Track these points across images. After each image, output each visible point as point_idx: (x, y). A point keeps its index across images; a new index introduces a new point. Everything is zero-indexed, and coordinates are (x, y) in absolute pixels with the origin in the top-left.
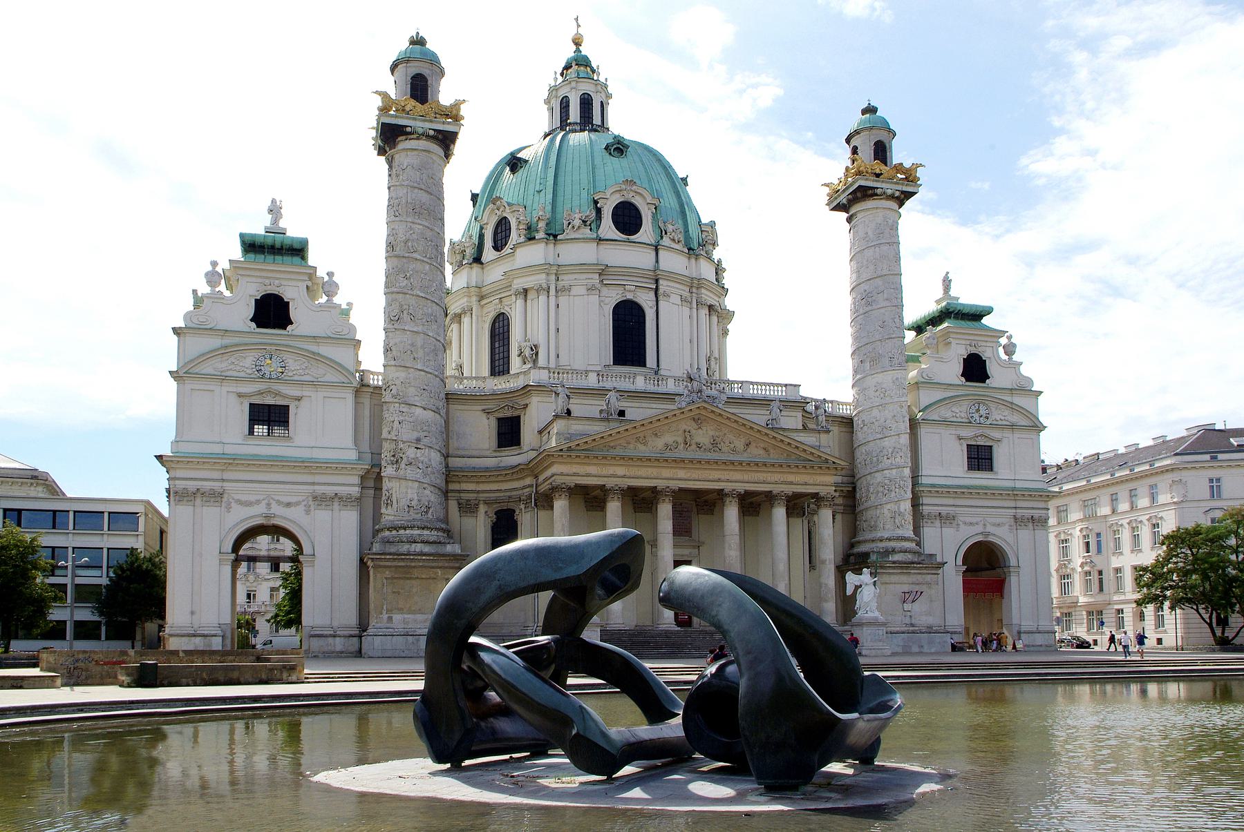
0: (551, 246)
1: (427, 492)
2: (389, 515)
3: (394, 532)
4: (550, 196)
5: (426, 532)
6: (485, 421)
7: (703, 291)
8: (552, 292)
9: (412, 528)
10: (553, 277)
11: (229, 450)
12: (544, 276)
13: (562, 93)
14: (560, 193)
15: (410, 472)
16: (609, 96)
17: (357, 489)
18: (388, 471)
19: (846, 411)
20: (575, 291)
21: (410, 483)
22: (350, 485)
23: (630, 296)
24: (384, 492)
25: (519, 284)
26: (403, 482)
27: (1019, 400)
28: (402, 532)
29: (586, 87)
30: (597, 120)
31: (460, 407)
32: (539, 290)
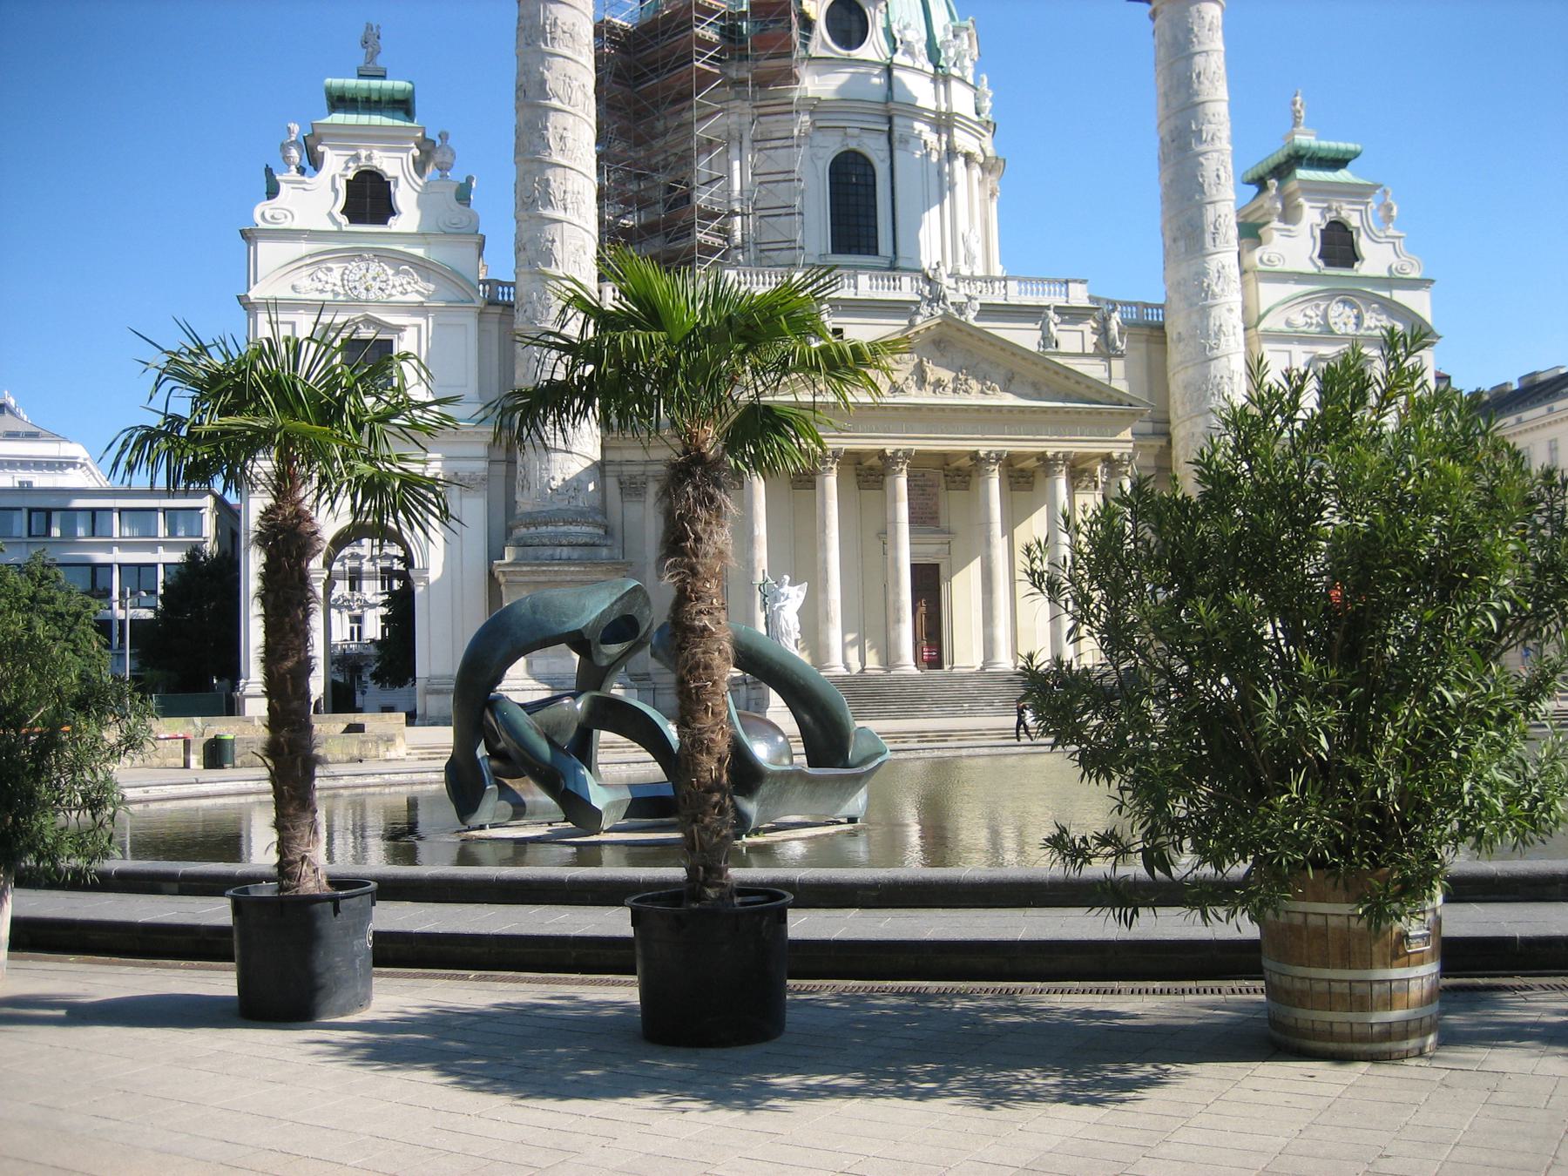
5: (573, 529)
17: (483, 465)
19: (1153, 316)
23: (853, 145)
24: (519, 469)
27: (1400, 296)
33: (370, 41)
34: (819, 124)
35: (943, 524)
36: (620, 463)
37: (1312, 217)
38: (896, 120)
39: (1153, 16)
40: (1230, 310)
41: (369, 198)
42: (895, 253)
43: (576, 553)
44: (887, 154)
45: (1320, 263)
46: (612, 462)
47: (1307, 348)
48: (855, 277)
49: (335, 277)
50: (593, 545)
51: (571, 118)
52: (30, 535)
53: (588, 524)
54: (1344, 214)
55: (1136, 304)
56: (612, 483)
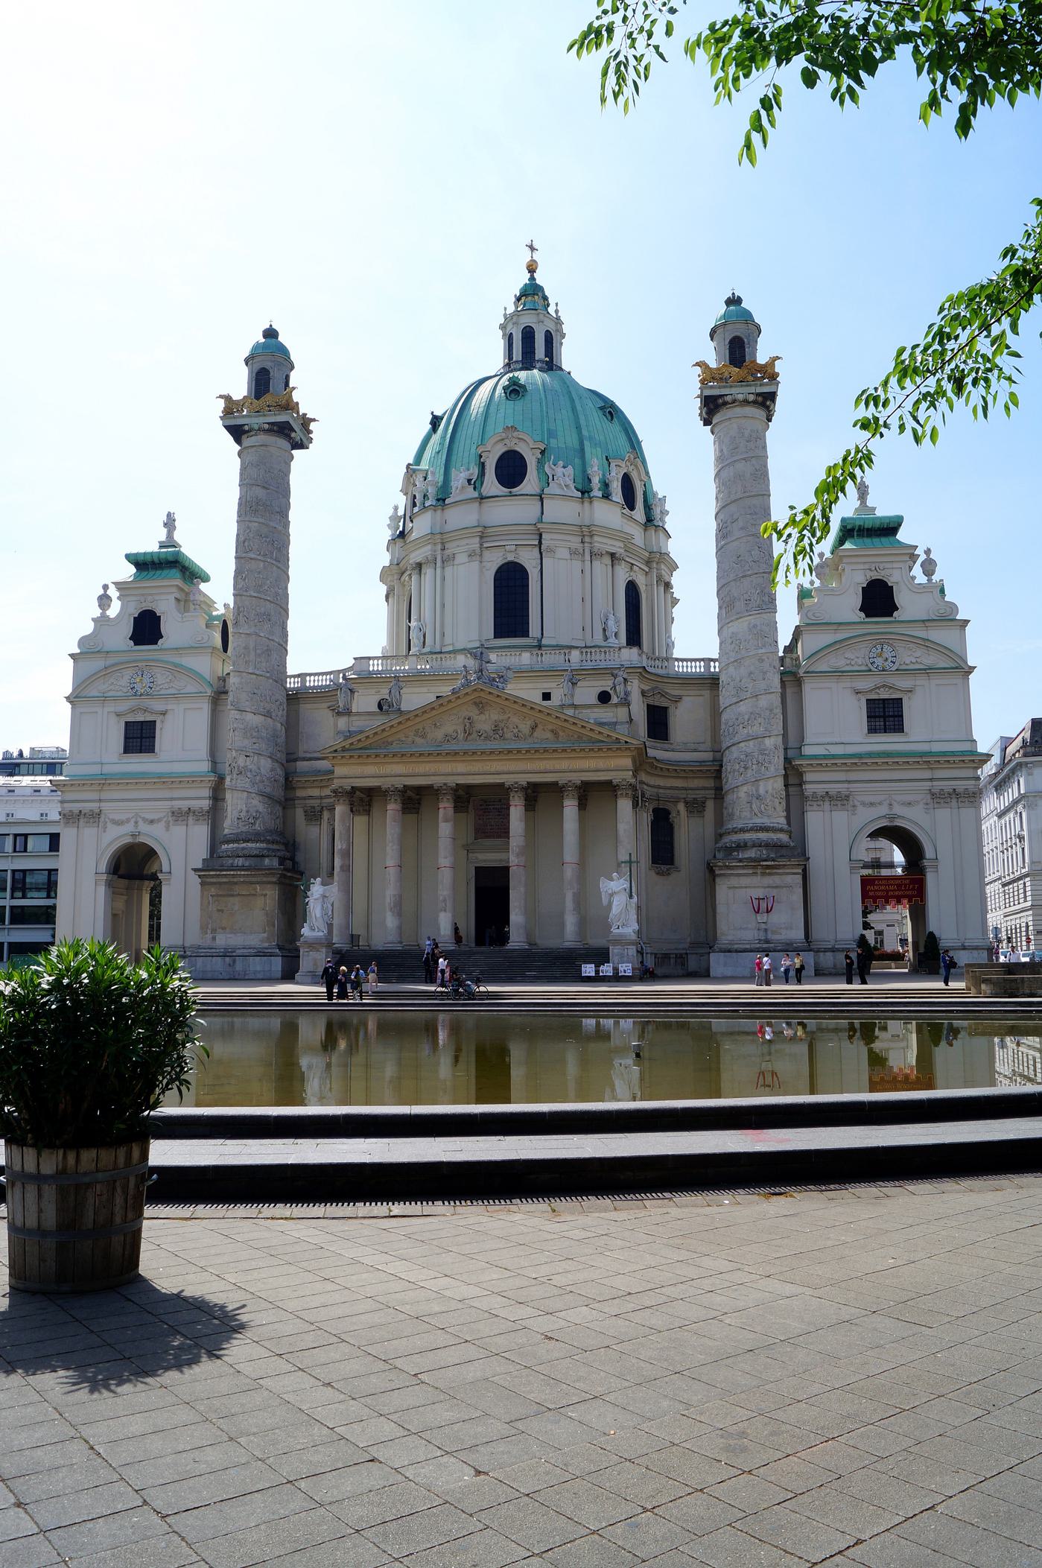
0: (439, 512)
2: (228, 826)
7: (596, 538)
8: (439, 564)
10: (439, 547)
11: (107, 769)
12: (429, 547)
13: (508, 332)
14: (455, 452)
15: (243, 782)
16: (558, 321)
19: (715, 668)
20: (461, 558)
23: (511, 558)
25: (416, 556)
26: (236, 794)
27: (937, 635)
29: (528, 320)
31: (308, 706)
32: (428, 562)
33: (170, 523)
36: (305, 798)
37: (858, 578)
40: (761, 661)
41: (147, 628)
45: (863, 615)
46: (299, 798)
47: (849, 685)
49: (124, 681)
52: (15, 851)
53: (262, 842)
54: (883, 573)
56: (299, 813)
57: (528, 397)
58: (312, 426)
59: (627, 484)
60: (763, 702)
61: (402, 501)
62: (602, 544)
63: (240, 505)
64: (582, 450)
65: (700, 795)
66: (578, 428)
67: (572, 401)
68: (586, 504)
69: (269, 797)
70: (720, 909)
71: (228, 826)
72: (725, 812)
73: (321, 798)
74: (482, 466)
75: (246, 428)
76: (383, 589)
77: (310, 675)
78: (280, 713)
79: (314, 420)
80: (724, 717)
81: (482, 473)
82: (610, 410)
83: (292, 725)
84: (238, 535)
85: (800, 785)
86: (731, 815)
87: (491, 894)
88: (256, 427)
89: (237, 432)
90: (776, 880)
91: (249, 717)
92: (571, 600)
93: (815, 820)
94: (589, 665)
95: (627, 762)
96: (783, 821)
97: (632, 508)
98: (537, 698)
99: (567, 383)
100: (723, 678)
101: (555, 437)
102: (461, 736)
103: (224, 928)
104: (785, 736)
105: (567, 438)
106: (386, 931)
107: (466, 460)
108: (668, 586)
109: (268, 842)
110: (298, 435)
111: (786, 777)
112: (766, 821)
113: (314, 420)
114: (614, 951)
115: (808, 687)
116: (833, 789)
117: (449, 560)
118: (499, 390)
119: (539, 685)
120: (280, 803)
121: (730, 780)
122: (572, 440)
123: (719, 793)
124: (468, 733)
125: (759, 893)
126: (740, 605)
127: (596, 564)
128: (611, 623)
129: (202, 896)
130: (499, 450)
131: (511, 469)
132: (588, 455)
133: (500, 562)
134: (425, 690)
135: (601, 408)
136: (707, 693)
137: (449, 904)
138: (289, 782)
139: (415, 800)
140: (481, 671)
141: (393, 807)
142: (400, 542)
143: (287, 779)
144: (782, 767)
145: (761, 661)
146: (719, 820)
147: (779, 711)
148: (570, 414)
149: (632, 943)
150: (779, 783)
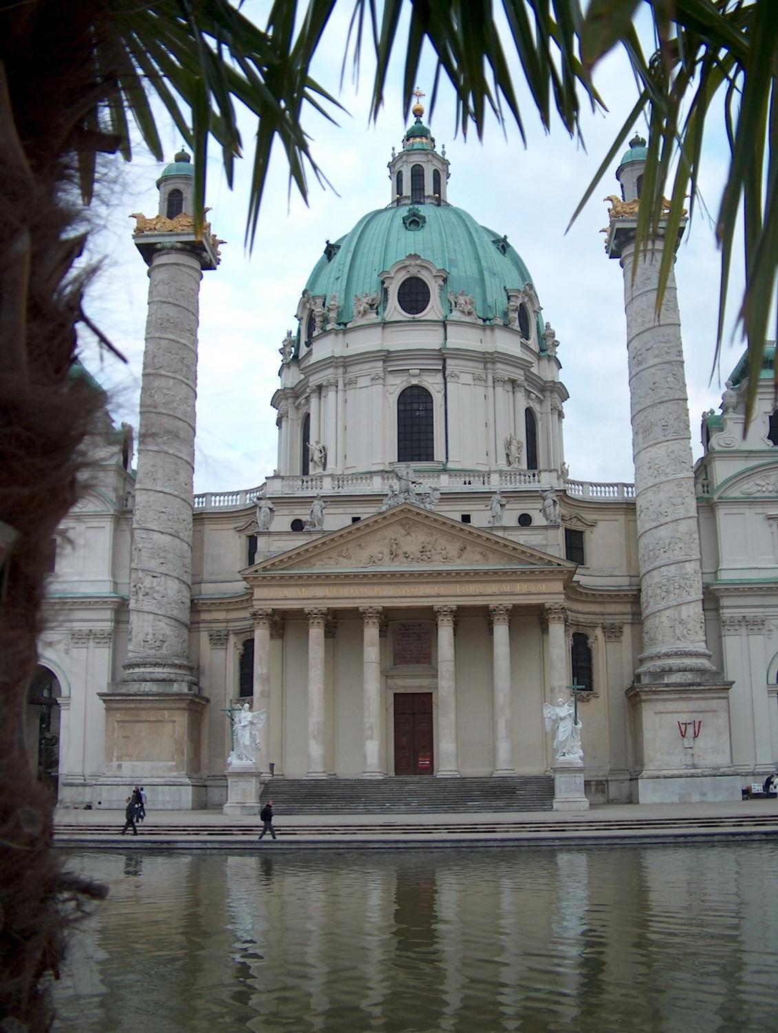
0: (341, 336)
1: (162, 624)
3: (131, 671)
4: (344, 283)
6: (239, 541)
7: (499, 365)
9: (144, 665)
10: (341, 370)
12: (331, 370)
13: (397, 168)
14: (355, 278)
15: (148, 605)
16: (446, 163)
18: (132, 604)
19: (629, 494)
20: (363, 382)
21: (146, 616)
22: (102, 621)
23: (415, 381)
25: (315, 380)
26: (142, 616)
28: (137, 670)
29: (416, 159)
30: (429, 189)
34: (389, 369)
35: (433, 662)
38: (448, 361)
39: (622, 265)
42: (447, 458)
43: (154, 688)
44: (443, 386)
47: (760, 511)
48: (439, 476)
50: (170, 681)
51: (171, 382)
55: (616, 485)
57: (426, 225)
58: (220, 248)
59: (523, 312)
60: (684, 527)
61: (294, 326)
62: (505, 371)
63: (149, 322)
64: (482, 280)
65: (617, 620)
66: (478, 258)
67: (470, 233)
68: (488, 332)
69: (176, 620)
70: (648, 735)
71: (133, 650)
72: (646, 637)
73: (228, 621)
74: (386, 291)
75: (159, 246)
76: (274, 413)
77: (216, 495)
78: (187, 534)
79: (222, 242)
80: (642, 542)
81: (386, 299)
82: (502, 245)
83: (197, 546)
84: (146, 353)
85: (717, 609)
86: (653, 641)
87: (413, 721)
88: (169, 245)
89: (148, 252)
90: (702, 705)
91: (157, 536)
92: (473, 425)
93: (733, 644)
94: (509, 487)
95: (559, 586)
96: (701, 647)
97: (526, 336)
98: (460, 519)
99: (461, 216)
100: (641, 503)
101: (456, 266)
102: (387, 558)
103: (130, 756)
104: (701, 560)
105: (464, 269)
106: (309, 761)
107: (367, 287)
108: (561, 415)
109: (174, 666)
110: (208, 256)
111: (703, 600)
112: (691, 648)
113: (222, 242)
114: (560, 780)
115: (721, 513)
116: (750, 613)
117: (350, 383)
118: (399, 222)
119: (458, 508)
120: (186, 626)
121: (651, 603)
122: (472, 270)
123: (638, 619)
124: (394, 555)
125: (685, 718)
126: (657, 430)
127: (499, 390)
128: (513, 448)
129: (107, 722)
130: (402, 277)
131: (414, 296)
132: (487, 283)
133: (405, 385)
134: (340, 511)
135: (494, 242)
136: (621, 518)
137: (376, 732)
138: (195, 606)
139: (340, 624)
140: (407, 491)
141: (316, 633)
142: (294, 369)
143: (192, 601)
144: (701, 592)
145: (680, 486)
146: (639, 644)
147: (696, 536)
148: (469, 246)
149: (580, 770)
150: (698, 608)
